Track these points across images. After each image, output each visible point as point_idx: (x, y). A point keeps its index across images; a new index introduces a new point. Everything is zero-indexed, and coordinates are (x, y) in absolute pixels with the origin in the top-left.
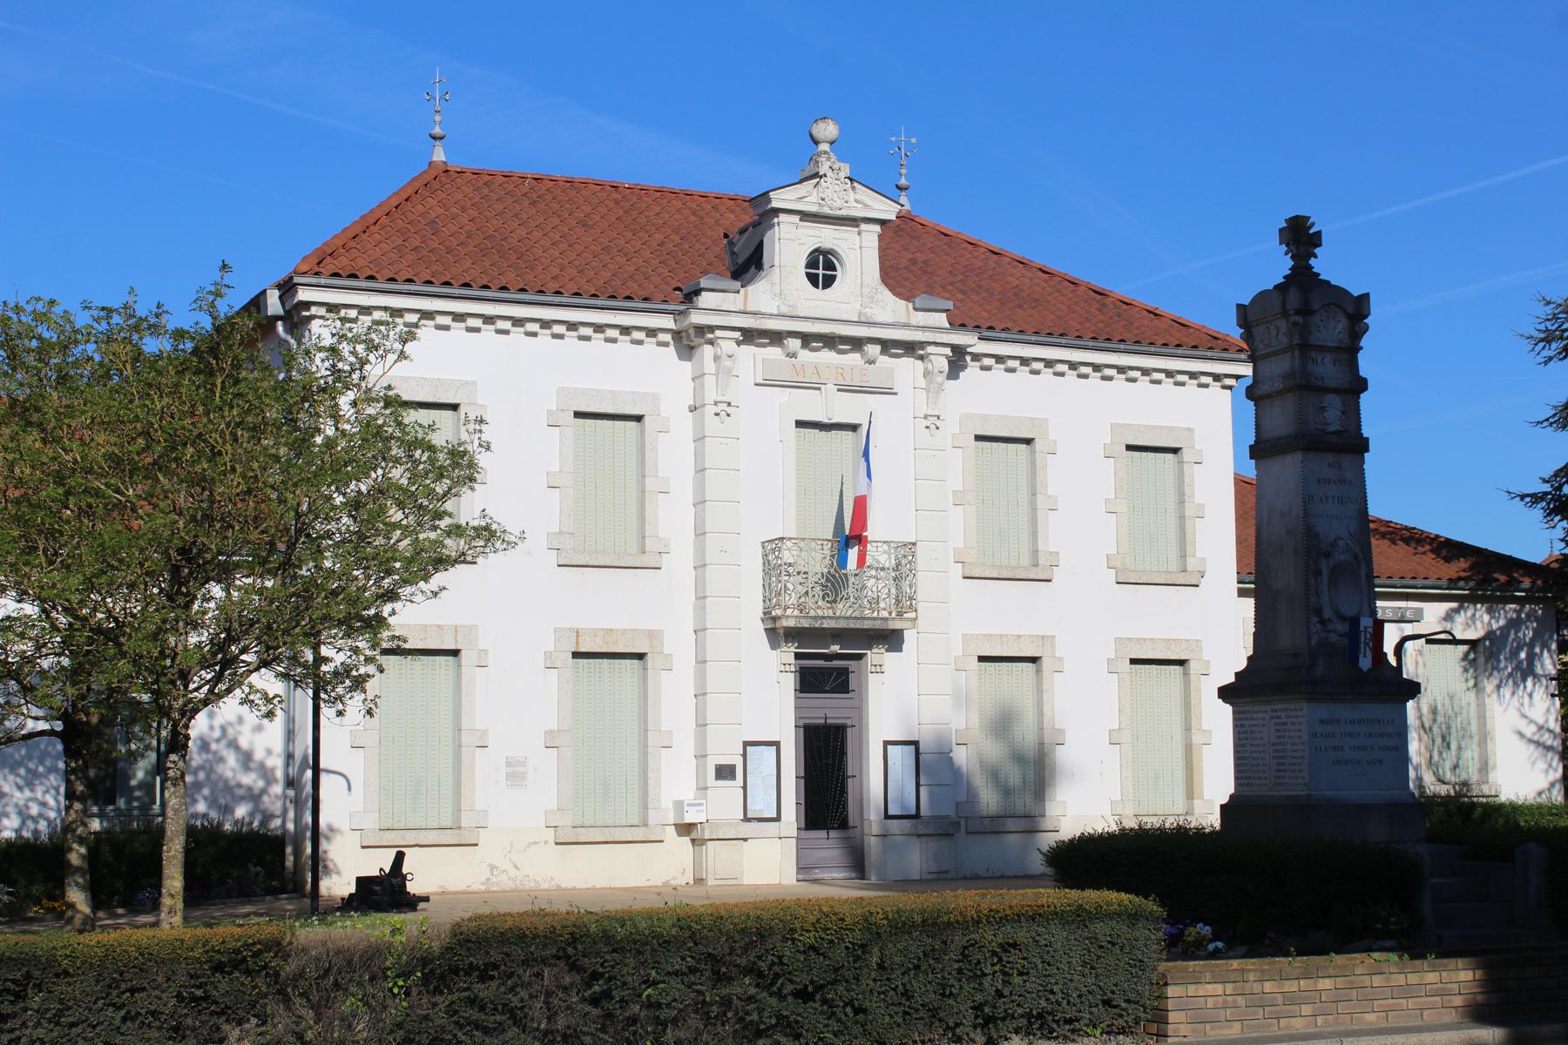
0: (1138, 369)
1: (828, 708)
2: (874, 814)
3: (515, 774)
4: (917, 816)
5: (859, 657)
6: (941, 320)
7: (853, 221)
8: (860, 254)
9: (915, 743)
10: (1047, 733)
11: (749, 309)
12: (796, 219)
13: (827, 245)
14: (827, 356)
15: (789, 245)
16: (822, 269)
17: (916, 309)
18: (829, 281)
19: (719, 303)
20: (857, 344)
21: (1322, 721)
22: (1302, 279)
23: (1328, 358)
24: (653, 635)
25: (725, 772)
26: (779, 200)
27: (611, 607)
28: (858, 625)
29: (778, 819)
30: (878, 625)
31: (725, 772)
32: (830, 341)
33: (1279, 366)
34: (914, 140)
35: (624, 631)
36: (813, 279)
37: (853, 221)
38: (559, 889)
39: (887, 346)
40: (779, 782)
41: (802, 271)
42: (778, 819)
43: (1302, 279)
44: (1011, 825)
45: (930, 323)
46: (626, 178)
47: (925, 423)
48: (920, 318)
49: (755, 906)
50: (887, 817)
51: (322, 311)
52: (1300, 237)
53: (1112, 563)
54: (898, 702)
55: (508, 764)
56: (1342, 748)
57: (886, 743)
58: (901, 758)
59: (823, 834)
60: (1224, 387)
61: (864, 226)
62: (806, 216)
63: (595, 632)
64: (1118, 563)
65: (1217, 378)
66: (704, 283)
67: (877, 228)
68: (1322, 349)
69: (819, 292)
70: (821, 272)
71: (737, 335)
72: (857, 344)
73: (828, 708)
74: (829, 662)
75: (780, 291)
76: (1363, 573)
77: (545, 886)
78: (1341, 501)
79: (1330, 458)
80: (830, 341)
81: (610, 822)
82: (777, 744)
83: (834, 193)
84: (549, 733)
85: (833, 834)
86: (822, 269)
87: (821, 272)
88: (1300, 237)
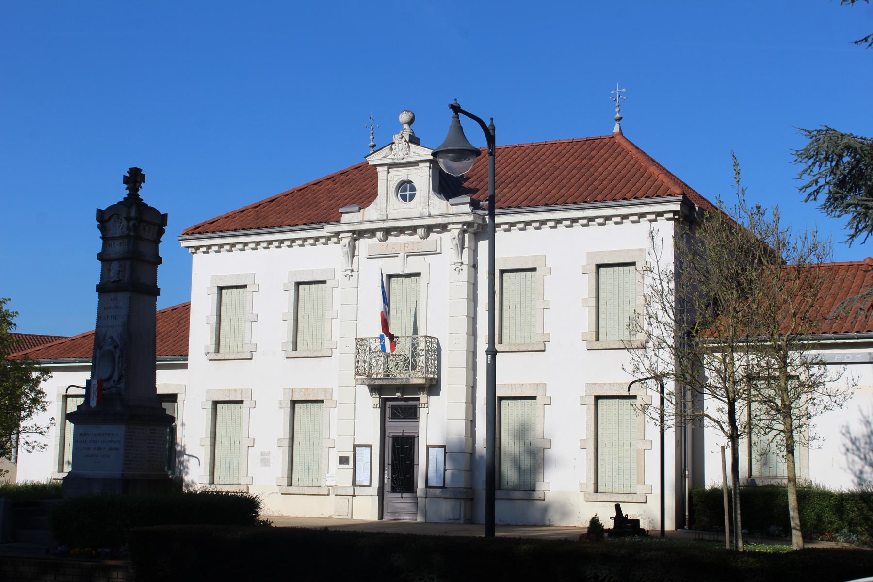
0: (601, 217)
1: (399, 427)
2: (421, 485)
3: (265, 460)
4: (443, 487)
5: (418, 399)
6: (467, 208)
7: (416, 163)
8: (422, 177)
9: (444, 446)
10: (508, 443)
11: (365, 219)
12: (385, 168)
13: (405, 179)
14: (404, 238)
15: (387, 181)
16: (406, 190)
17: (452, 205)
18: (412, 197)
19: (351, 219)
20: (413, 229)
21: (81, 434)
22: (133, 199)
23: (117, 242)
24: (325, 390)
25: (343, 460)
26: (373, 160)
27: (307, 378)
28: (394, 382)
29: (370, 486)
30: (404, 382)
31: (343, 460)
32: (401, 230)
33: (117, 248)
34: (624, 90)
35: (313, 389)
36: (404, 198)
37: (416, 163)
38: (282, 516)
39: (429, 229)
40: (369, 468)
41: (418, 193)
42: (370, 486)
43: (133, 199)
44: (518, 494)
45: (460, 211)
46: (526, 141)
47: (455, 267)
48: (454, 209)
49: (562, 537)
50: (427, 486)
51: (194, 250)
52: (135, 178)
53: (585, 338)
54: (440, 423)
55: (262, 455)
56: (88, 449)
57: (428, 447)
58: (437, 455)
59: (399, 495)
60: (668, 219)
61: (421, 165)
62: (391, 166)
63: (301, 389)
64: (588, 338)
65: (660, 214)
66: (341, 210)
67: (428, 164)
68: (113, 238)
69: (408, 204)
70: (408, 193)
71: (350, 234)
72: (413, 229)
73: (399, 427)
74: (399, 401)
75: (385, 207)
76: (117, 355)
77: (276, 514)
78: (115, 317)
79: (112, 295)
80: (401, 230)
81: (310, 485)
82: (371, 446)
83: (401, 150)
84: (279, 440)
85: (405, 495)
86: (406, 190)
87: (408, 193)
88: (135, 178)
